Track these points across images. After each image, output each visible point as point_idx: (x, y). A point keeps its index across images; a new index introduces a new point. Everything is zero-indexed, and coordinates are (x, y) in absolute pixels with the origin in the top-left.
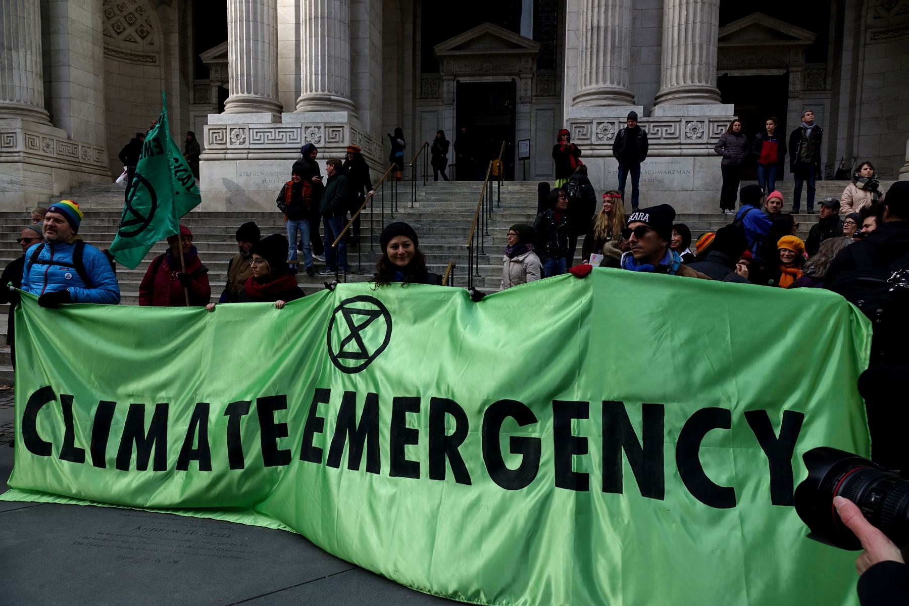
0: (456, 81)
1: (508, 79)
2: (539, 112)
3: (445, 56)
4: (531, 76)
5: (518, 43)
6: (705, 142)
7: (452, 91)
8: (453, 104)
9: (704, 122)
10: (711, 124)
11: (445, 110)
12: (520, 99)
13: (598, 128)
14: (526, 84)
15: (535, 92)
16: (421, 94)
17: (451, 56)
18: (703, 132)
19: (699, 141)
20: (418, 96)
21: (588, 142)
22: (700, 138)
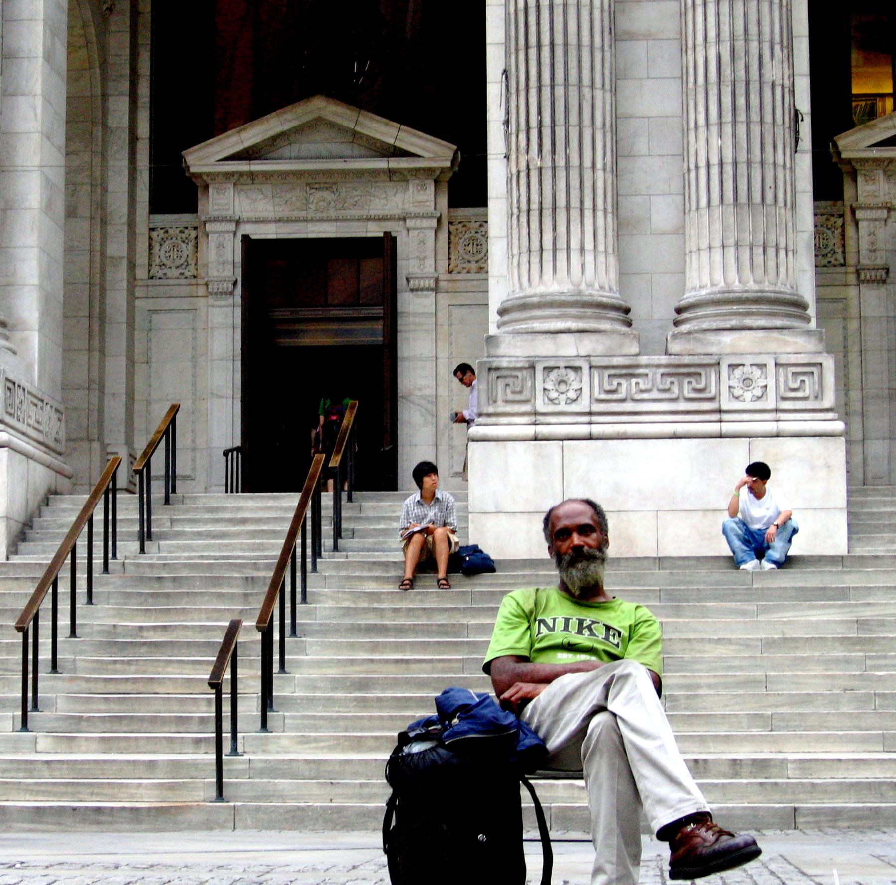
0: (239, 238)
1: (374, 230)
2: (457, 312)
3: (213, 176)
4: (434, 223)
5: (398, 144)
6: (771, 405)
7: (230, 259)
8: (232, 293)
9: (765, 365)
10: (781, 370)
11: (213, 306)
12: (408, 280)
13: (547, 379)
14: (423, 242)
15: (447, 262)
16: (150, 265)
17: (228, 175)
18: (766, 387)
19: (758, 405)
20: (141, 273)
21: (526, 408)
22: (759, 398)
